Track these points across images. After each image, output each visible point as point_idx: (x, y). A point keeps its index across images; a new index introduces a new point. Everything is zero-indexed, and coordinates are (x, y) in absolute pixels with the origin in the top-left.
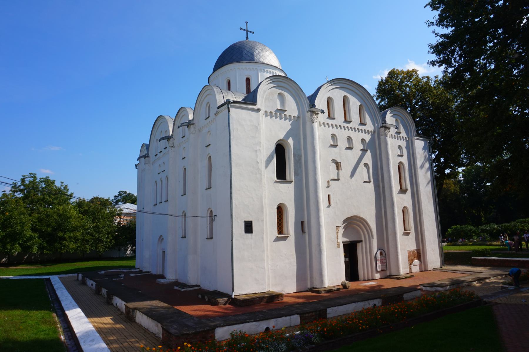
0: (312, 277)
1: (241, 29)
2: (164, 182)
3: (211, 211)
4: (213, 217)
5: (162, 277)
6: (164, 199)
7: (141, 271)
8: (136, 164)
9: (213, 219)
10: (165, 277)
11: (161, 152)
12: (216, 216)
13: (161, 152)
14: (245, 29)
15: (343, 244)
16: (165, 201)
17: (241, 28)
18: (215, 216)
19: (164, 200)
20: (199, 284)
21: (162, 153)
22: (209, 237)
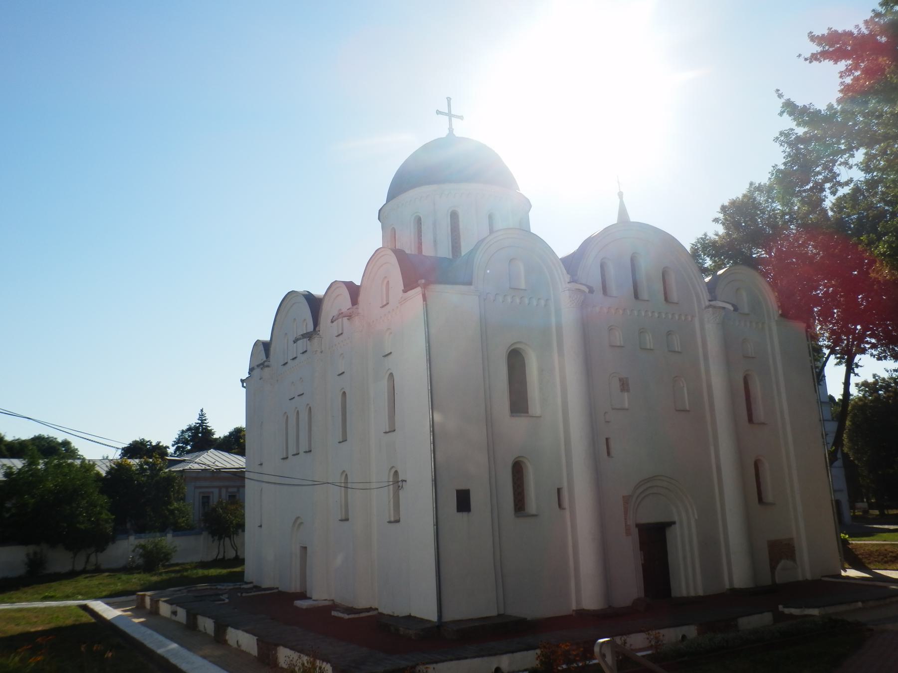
0: (578, 592)
1: (438, 112)
2: (304, 416)
3: (396, 472)
4: (400, 484)
5: (303, 596)
6: (303, 447)
7: (257, 588)
8: (243, 379)
9: (399, 487)
10: (308, 595)
11: (294, 359)
12: (406, 481)
13: (294, 359)
14: (447, 111)
15: (637, 530)
16: (306, 452)
17: (437, 110)
18: (403, 481)
19: (302, 449)
20: (375, 606)
21: (296, 361)
22: (392, 519)
